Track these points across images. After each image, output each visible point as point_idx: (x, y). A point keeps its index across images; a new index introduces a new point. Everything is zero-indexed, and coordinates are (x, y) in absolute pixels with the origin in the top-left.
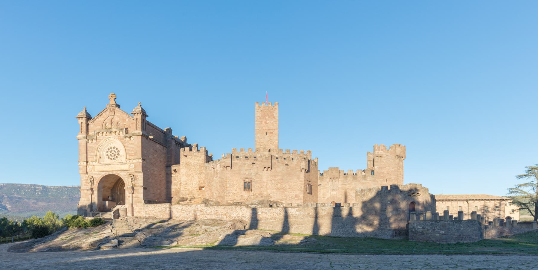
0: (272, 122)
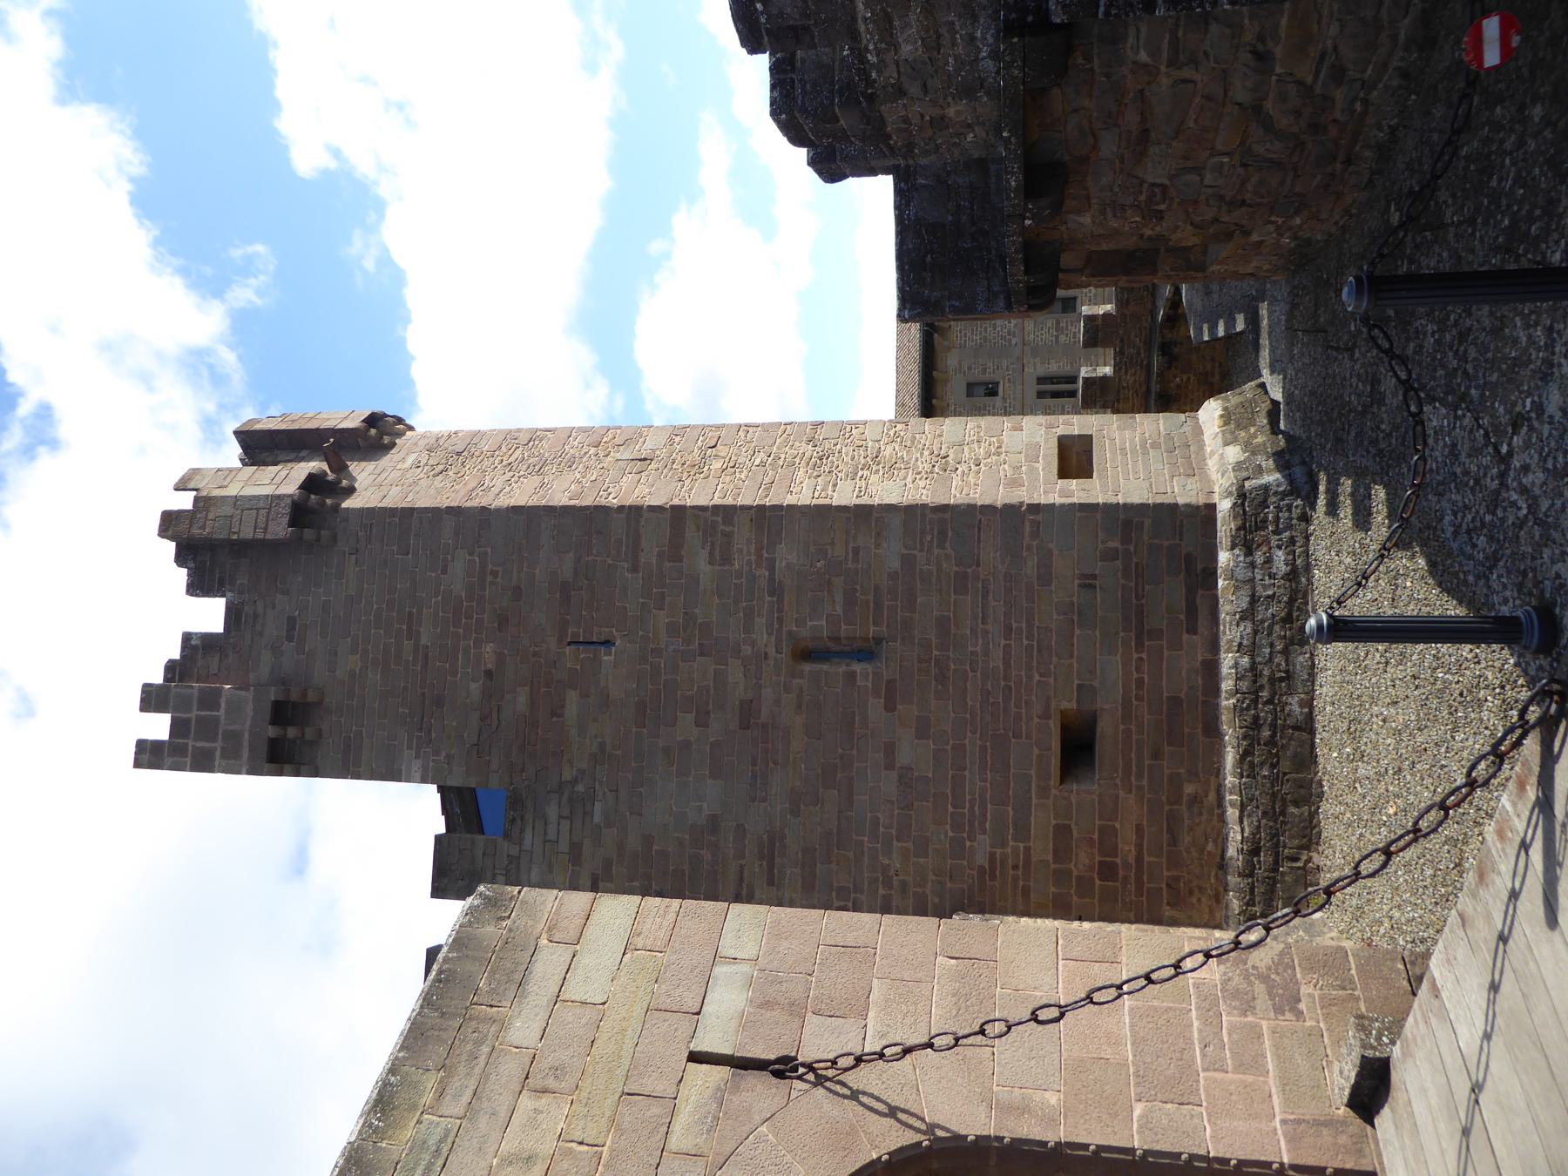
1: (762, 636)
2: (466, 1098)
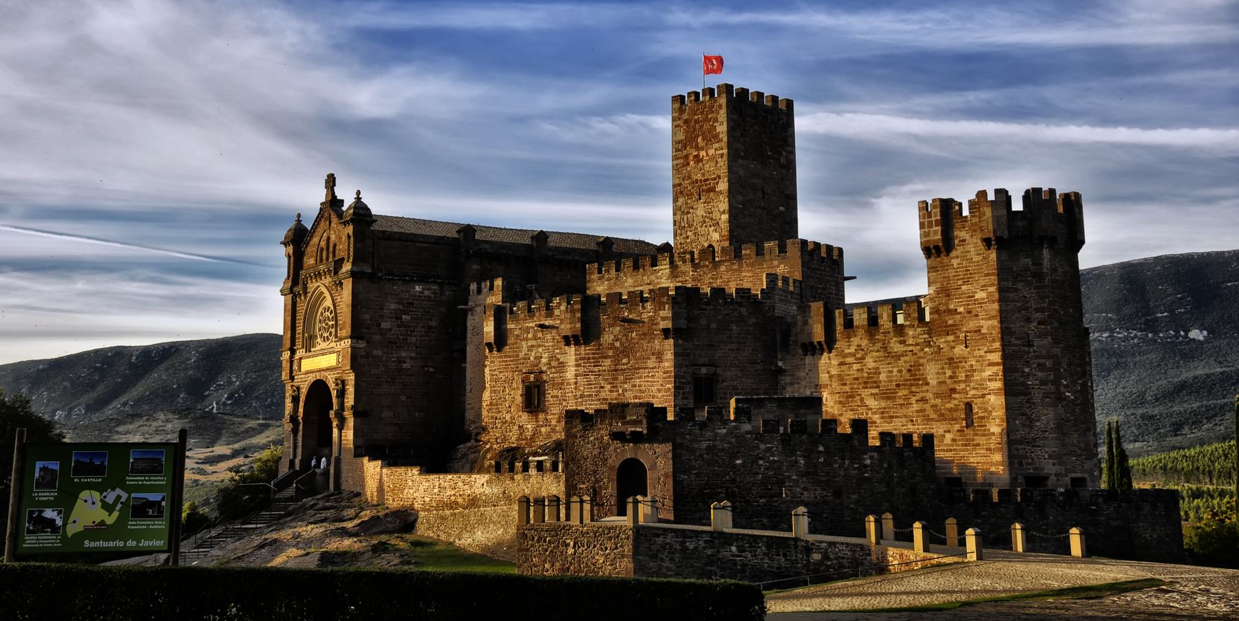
0: (711, 152)
1: (972, 392)
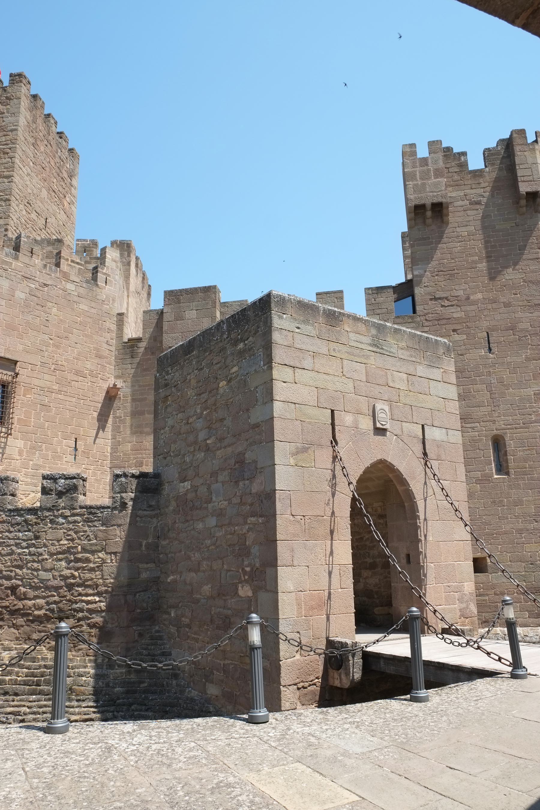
2: (402, 357)
